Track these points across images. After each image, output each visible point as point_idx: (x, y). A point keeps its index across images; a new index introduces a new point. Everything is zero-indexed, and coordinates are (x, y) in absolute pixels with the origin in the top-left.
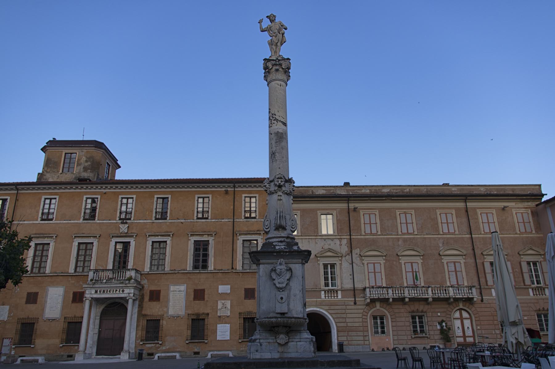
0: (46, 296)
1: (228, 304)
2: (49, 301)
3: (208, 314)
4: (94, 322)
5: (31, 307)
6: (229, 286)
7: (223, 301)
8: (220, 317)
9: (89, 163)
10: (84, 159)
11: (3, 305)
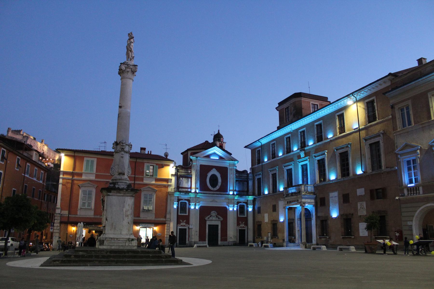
1: (364, 204)
3: (353, 214)
4: (298, 223)
6: (363, 189)
7: (361, 203)
8: (360, 216)
9: (295, 111)
10: (293, 108)
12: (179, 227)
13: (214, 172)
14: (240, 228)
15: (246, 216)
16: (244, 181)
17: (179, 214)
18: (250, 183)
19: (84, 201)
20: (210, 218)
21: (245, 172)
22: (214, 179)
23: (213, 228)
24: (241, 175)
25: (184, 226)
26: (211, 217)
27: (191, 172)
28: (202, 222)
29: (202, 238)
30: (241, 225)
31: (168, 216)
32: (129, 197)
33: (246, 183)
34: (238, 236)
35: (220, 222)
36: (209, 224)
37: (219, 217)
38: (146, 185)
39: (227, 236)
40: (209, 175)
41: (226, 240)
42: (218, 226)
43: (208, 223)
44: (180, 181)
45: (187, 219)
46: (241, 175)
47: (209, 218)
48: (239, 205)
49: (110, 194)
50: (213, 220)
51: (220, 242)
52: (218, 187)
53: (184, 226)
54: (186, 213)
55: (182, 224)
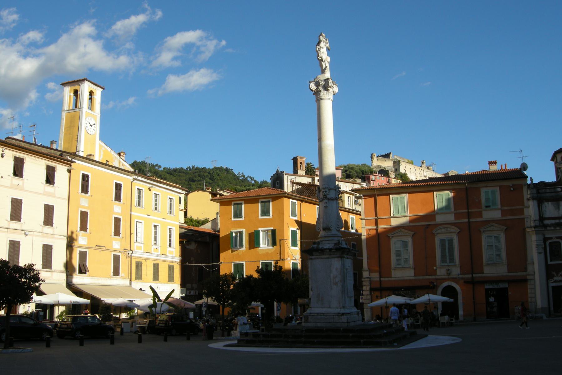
12: (552, 284)
17: (549, 262)
19: (398, 258)
31: (529, 268)
32: (336, 259)
44: (543, 209)
49: (313, 257)
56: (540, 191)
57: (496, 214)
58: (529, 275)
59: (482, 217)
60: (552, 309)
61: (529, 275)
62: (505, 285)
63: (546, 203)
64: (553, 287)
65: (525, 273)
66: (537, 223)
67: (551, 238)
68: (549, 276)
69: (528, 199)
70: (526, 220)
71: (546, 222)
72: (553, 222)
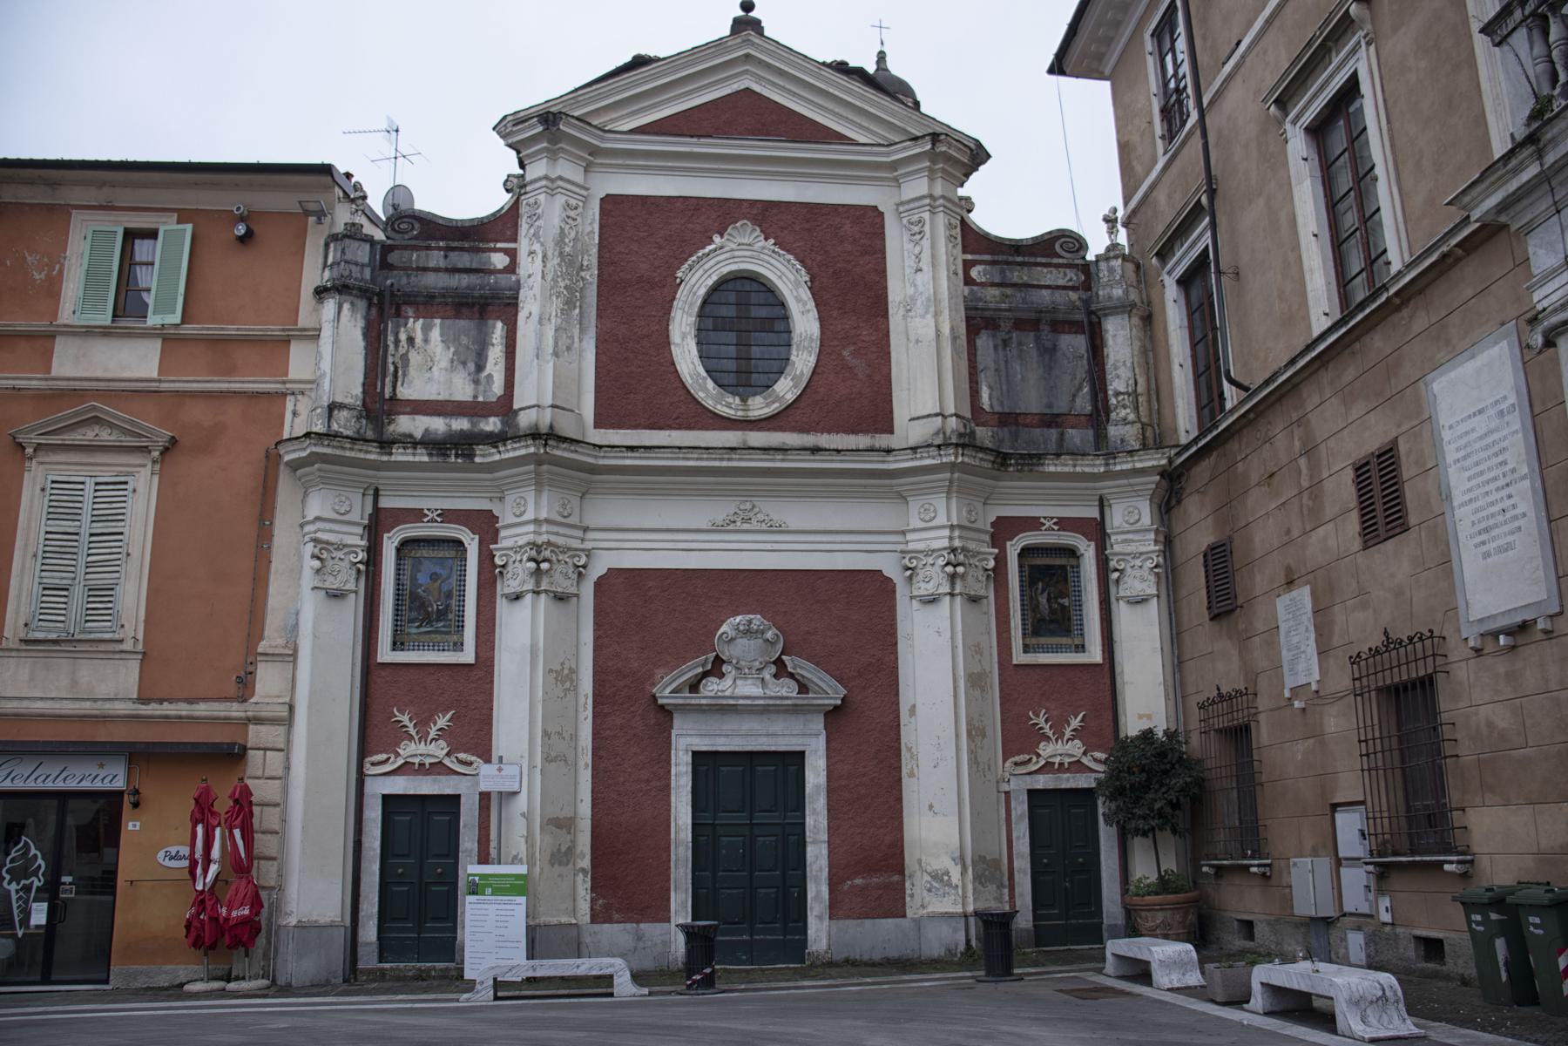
0: (1436, 444)
2: (1459, 482)
5: (1395, 560)
11: (1290, 584)
12: (379, 787)
13: (742, 251)
14: (1042, 782)
15: (1095, 654)
16: (1061, 325)
17: (385, 654)
18: (1120, 339)
20: (712, 686)
21: (1059, 246)
22: (742, 314)
23: (748, 788)
24: (1016, 276)
25: (438, 768)
26: (717, 668)
27: (512, 268)
28: (627, 720)
29: (623, 879)
30: (1047, 750)
31: (268, 681)
33: (1075, 343)
34: (1023, 864)
35: (818, 724)
36: (704, 745)
37: (807, 670)
38: (73, 394)
39: (901, 870)
40: (697, 280)
41: (891, 902)
42: (795, 760)
43: (687, 740)
45: (466, 701)
46: (1016, 276)
47: (694, 687)
48: (1013, 550)
50: (747, 700)
51: (819, 932)
52: (786, 390)
53: (438, 768)
54: (459, 646)
55: (410, 750)
56: (393, 258)
57: (137, 361)
58: (258, 721)
59: (48, 369)
60: (369, 932)
61: (258, 721)
62: (113, 777)
63: (416, 326)
64: (387, 799)
65: (235, 710)
66: (344, 423)
67: (417, 515)
68: (371, 734)
69: (321, 292)
70: (289, 406)
71: (406, 424)
72: (438, 425)
